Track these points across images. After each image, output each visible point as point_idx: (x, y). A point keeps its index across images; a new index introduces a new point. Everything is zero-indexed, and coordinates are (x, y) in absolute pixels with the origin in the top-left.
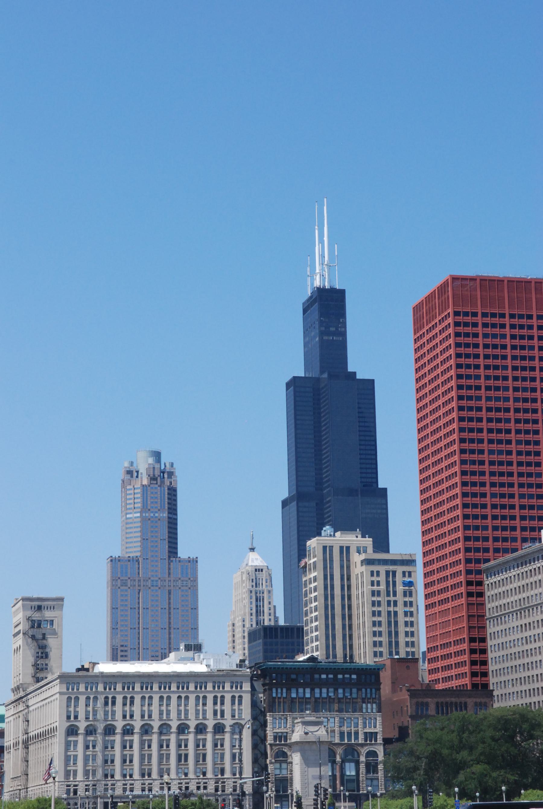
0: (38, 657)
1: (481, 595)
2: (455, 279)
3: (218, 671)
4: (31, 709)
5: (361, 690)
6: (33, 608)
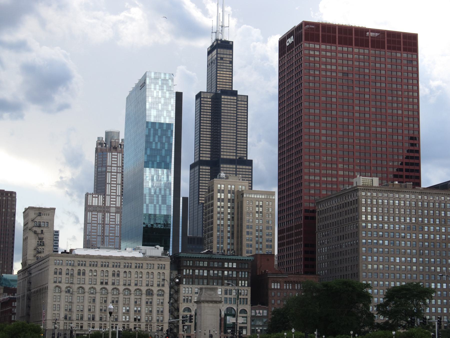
0: (38, 244)
1: (314, 218)
2: (306, 23)
3: (150, 257)
4: (33, 275)
5: (239, 272)
6: (36, 214)
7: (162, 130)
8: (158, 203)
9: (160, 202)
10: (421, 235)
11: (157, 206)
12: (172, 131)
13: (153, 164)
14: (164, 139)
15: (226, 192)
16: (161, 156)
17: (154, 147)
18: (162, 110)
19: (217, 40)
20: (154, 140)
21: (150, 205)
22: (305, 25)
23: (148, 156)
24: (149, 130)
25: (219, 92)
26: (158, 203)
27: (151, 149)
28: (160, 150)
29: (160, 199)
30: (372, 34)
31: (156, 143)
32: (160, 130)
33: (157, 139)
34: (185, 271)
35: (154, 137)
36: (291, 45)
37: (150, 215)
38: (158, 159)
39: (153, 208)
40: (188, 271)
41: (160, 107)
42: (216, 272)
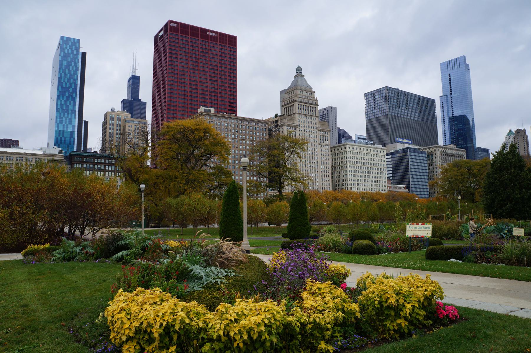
7: (70, 75)
8: (66, 123)
9: (67, 123)
10: (241, 146)
11: (66, 125)
12: (77, 76)
13: (63, 97)
14: (72, 81)
15: (115, 119)
16: (69, 92)
17: (64, 86)
18: (71, 62)
19: (132, 75)
20: (64, 81)
21: (60, 124)
22: (170, 23)
23: (60, 91)
24: (61, 74)
25: (132, 100)
26: (66, 123)
27: (62, 87)
28: (69, 88)
29: (68, 120)
30: (211, 34)
31: (66, 83)
32: (68, 75)
33: (66, 81)
34: (75, 165)
35: (64, 79)
36: (162, 36)
37: (60, 131)
38: (67, 93)
39: (62, 126)
40: (78, 165)
41: (69, 60)
42: (99, 166)
